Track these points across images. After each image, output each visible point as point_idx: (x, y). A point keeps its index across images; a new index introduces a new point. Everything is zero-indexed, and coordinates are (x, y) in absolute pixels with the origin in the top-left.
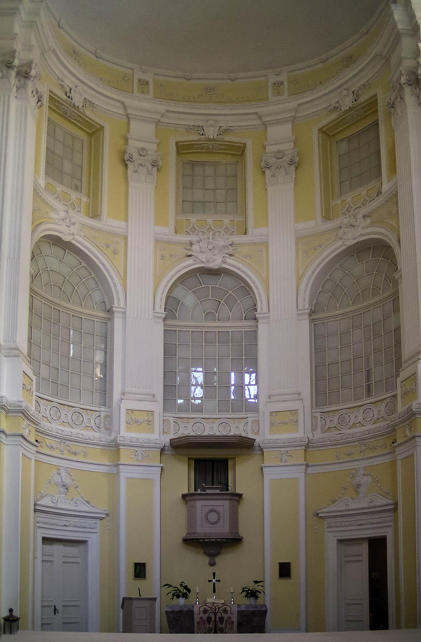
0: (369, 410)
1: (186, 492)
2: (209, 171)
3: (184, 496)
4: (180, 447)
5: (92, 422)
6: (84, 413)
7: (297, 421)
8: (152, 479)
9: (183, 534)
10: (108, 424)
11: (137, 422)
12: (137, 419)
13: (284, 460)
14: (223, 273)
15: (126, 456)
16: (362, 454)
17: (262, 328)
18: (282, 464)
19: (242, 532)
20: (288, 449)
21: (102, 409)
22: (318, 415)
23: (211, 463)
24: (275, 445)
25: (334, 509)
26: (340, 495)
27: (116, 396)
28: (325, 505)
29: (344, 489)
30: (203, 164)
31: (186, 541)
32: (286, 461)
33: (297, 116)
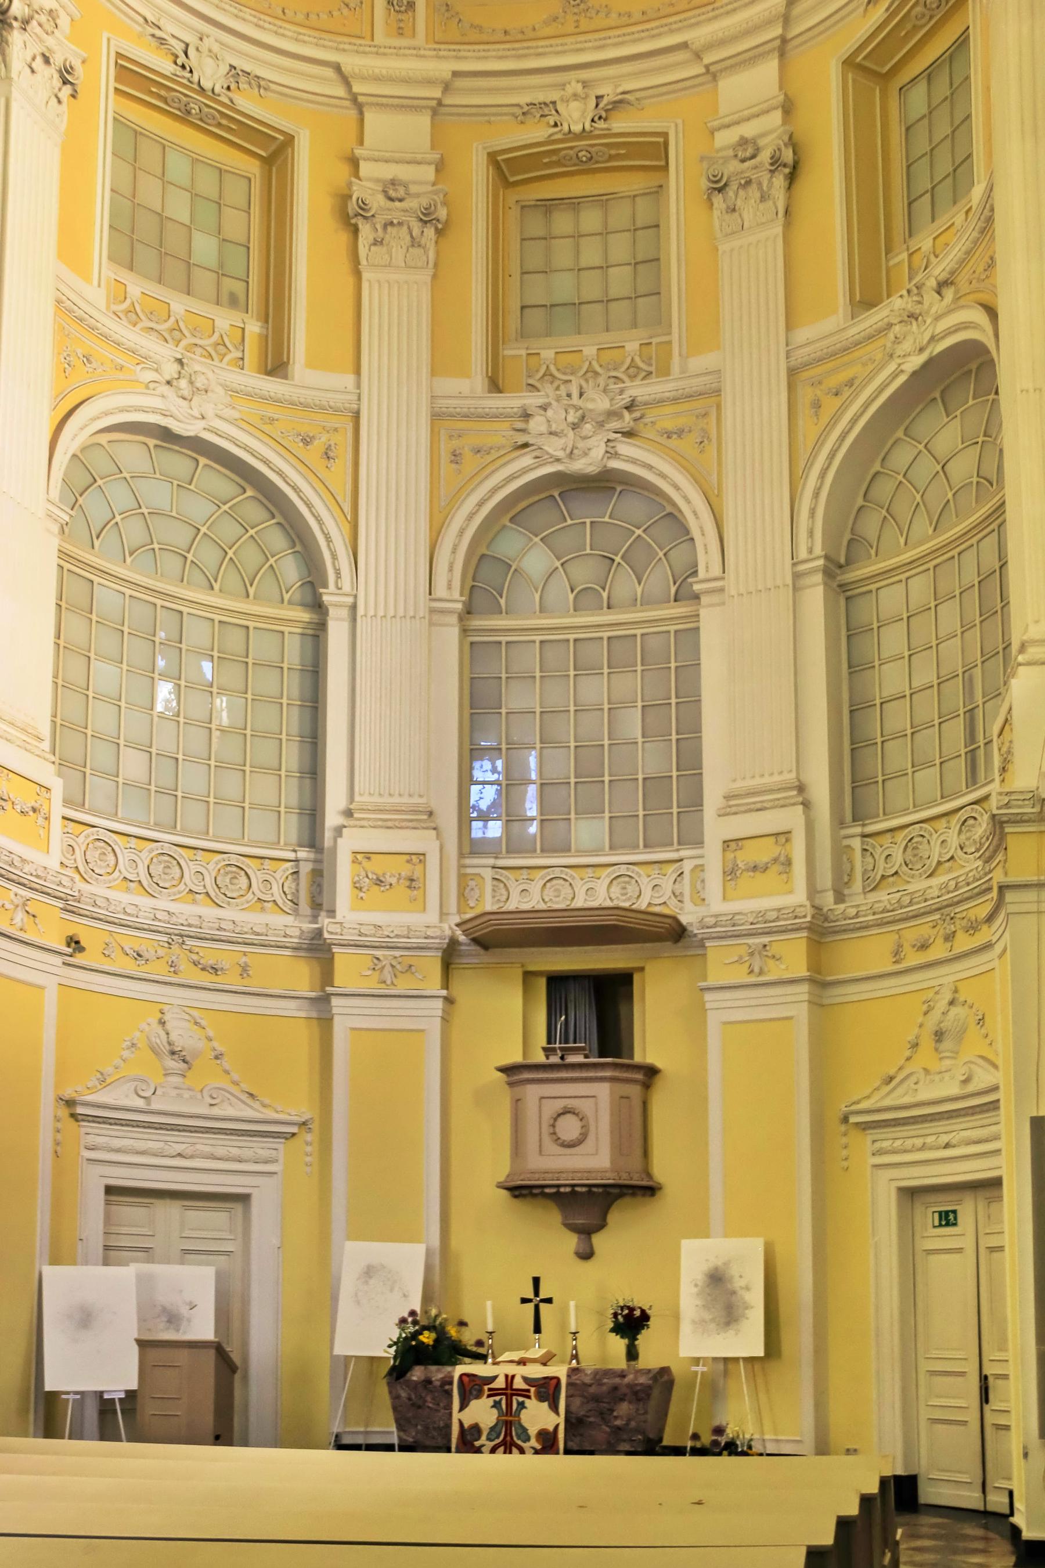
2: (591, 219)
4: (493, 939)
8: (422, 1031)
9: (502, 1170)
13: (756, 970)
14: (621, 483)
17: (712, 624)
18: (753, 979)
20: (765, 940)
30: (574, 204)
33: (790, 36)
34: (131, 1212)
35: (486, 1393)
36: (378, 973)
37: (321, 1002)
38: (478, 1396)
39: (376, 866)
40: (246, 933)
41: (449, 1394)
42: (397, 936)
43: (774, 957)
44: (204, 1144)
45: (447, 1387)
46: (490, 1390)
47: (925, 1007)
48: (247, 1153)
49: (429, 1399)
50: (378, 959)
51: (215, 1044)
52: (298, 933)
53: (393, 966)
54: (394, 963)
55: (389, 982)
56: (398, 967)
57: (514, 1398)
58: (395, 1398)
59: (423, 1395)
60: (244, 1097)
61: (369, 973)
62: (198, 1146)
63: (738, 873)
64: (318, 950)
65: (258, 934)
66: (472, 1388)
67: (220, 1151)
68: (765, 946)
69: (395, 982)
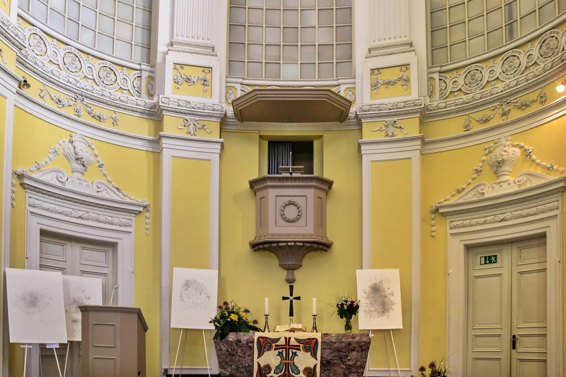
0: (512, 58)
1: (256, 176)
3: (253, 184)
5: (129, 84)
6: (118, 69)
7: (407, 80)
8: (210, 160)
10: (153, 86)
11: (188, 80)
12: (188, 76)
15: (171, 125)
16: (505, 117)
18: (387, 138)
19: (333, 234)
21: (143, 67)
22: (436, 76)
23: (290, 134)
24: (378, 114)
25: (462, 201)
26: (470, 181)
27: (161, 47)
28: (448, 197)
29: (477, 172)
31: (258, 247)
32: (393, 135)
34: (54, 248)
35: (274, 347)
36: (186, 128)
37: (156, 142)
38: (269, 350)
39: (187, 72)
40: (116, 100)
41: (251, 348)
42: (199, 108)
43: (400, 127)
44: (93, 213)
45: (250, 344)
46: (276, 346)
47: (487, 151)
48: (116, 220)
49: (239, 351)
50: (187, 120)
51: (99, 159)
52: (144, 104)
53: (195, 125)
54: (195, 123)
55: (192, 133)
56: (197, 125)
57: (285, 350)
58: (219, 350)
59: (236, 349)
60: (115, 190)
61: (183, 127)
62: (90, 214)
63: (379, 86)
64: (155, 114)
65: (123, 101)
66: (265, 345)
67: (102, 218)
68: (395, 122)
69: (196, 133)
